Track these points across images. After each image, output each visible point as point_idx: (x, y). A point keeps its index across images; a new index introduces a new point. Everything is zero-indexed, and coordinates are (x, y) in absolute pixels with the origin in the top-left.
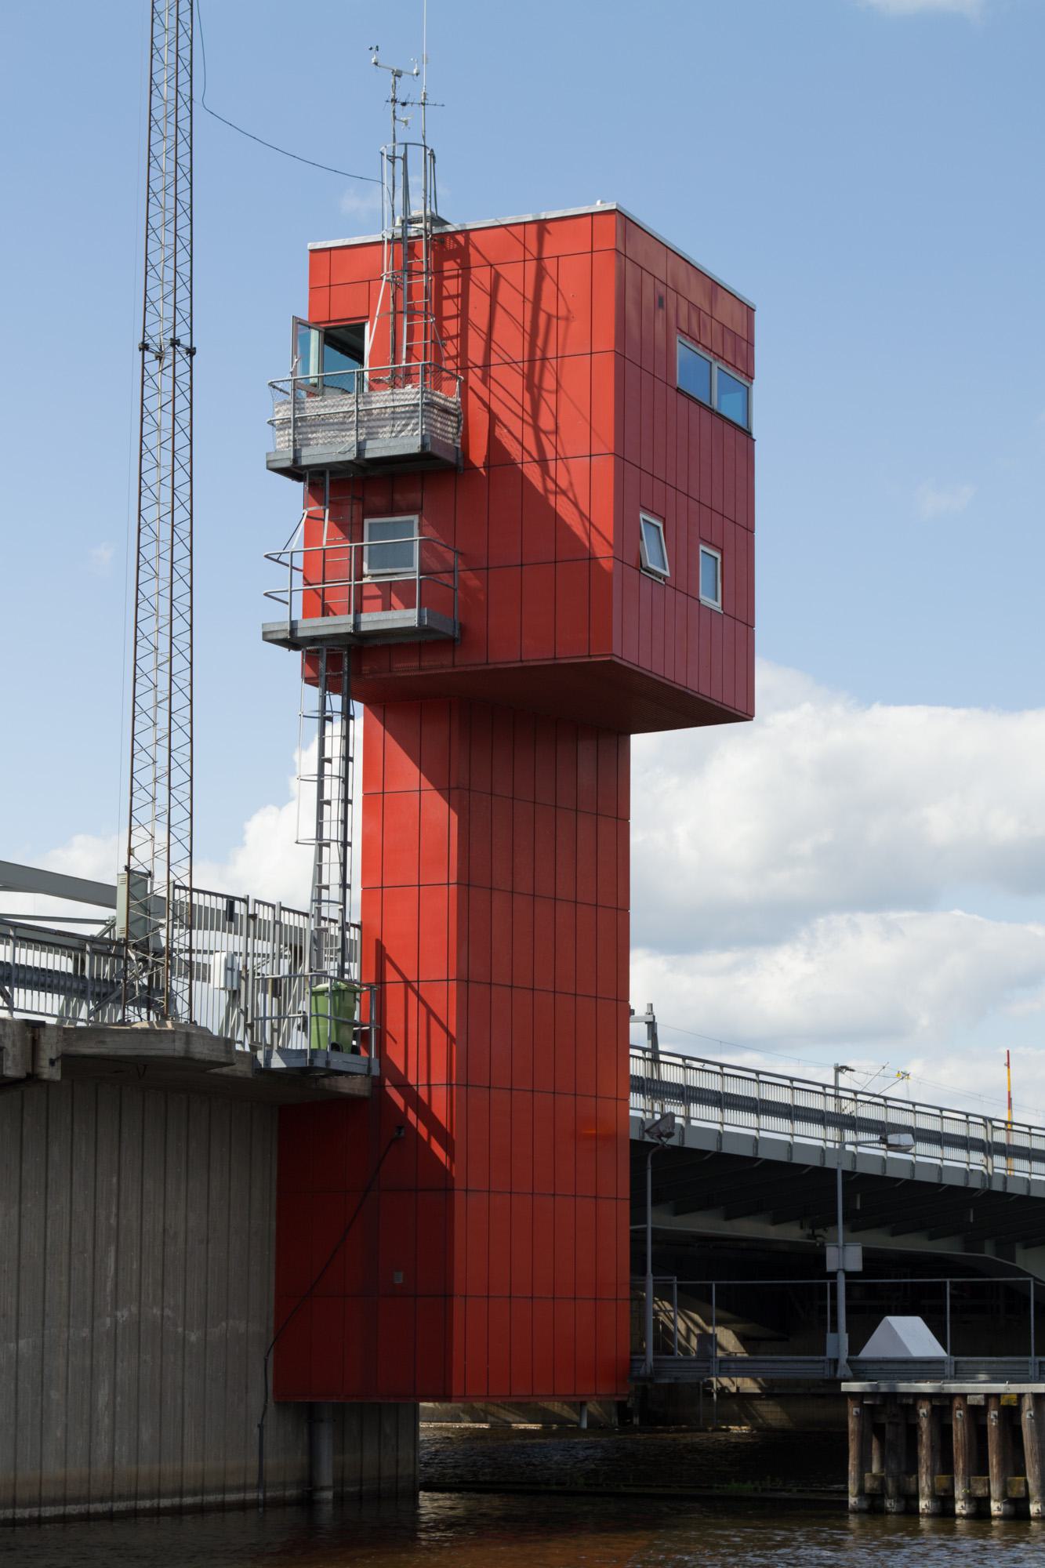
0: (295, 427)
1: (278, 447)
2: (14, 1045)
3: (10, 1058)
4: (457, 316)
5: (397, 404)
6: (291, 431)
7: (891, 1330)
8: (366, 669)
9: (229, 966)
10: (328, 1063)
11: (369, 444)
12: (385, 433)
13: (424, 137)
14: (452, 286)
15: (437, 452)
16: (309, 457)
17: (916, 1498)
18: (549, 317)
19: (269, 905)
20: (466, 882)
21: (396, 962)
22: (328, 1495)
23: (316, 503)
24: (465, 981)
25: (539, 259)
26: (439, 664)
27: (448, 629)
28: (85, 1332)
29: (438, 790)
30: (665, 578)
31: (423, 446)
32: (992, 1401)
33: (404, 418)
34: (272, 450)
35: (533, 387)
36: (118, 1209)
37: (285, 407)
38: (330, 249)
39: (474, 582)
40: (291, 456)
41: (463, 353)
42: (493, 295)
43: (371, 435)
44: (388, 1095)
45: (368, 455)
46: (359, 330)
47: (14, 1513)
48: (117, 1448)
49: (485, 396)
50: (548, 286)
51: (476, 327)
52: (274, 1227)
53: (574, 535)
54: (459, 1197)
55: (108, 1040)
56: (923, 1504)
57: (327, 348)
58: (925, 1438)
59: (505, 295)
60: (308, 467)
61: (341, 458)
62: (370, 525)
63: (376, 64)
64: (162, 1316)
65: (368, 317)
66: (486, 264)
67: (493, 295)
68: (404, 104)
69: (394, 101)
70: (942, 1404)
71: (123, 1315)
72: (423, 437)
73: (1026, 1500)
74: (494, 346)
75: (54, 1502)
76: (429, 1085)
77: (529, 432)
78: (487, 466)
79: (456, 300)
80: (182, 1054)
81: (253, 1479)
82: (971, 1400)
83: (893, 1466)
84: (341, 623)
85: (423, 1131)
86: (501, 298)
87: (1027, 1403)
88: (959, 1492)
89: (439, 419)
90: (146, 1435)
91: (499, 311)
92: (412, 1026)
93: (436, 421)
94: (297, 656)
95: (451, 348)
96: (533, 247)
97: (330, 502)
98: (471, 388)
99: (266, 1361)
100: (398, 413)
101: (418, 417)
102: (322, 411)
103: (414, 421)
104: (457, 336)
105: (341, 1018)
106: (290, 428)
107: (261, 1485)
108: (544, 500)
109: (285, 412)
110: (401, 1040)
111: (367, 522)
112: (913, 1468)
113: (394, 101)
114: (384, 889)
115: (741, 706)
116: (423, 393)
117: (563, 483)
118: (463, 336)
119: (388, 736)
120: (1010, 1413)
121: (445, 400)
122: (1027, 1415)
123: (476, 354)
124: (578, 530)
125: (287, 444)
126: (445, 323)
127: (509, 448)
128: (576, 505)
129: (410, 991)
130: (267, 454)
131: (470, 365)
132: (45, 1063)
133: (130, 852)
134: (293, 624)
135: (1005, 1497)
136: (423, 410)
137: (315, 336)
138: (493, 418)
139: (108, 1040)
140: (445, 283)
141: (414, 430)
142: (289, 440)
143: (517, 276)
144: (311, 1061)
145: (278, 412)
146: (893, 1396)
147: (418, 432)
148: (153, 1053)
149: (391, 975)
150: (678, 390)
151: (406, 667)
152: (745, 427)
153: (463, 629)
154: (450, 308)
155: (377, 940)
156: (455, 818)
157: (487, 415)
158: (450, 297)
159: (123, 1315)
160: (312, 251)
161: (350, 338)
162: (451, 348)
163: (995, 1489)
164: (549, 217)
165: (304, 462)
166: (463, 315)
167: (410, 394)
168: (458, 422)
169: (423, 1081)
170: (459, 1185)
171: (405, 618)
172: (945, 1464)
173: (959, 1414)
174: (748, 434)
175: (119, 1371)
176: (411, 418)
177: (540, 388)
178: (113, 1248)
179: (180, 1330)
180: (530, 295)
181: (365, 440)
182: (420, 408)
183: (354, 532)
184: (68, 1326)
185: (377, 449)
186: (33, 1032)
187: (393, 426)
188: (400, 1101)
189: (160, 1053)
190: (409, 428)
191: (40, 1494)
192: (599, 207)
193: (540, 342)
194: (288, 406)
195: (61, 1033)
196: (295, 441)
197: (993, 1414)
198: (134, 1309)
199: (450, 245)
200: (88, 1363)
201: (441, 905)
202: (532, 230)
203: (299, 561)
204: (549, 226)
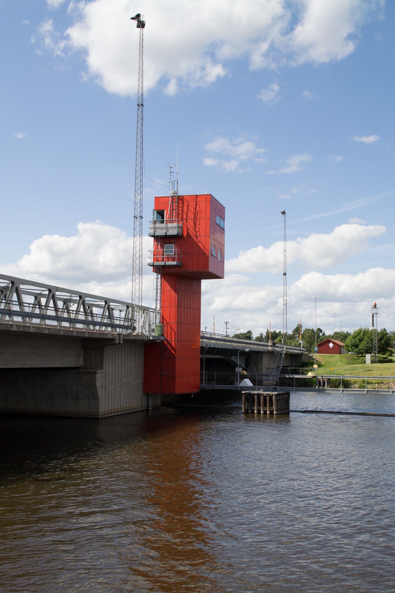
7: (246, 382)
8: (164, 270)
12: (170, 231)
14: (181, 205)
16: (157, 234)
17: (254, 410)
18: (198, 211)
20: (178, 306)
22: (151, 408)
24: (178, 323)
25: (196, 202)
26: (178, 270)
27: (180, 265)
28: (120, 384)
29: (174, 290)
32: (268, 395)
35: (195, 224)
39: (184, 256)
43: (168, 231)
45: (167, 234)
46: (164, 211)
49: (186, 224)
50: (198, 207)
51: (185, 213)
53: (202, 250)
54: (177, 359)
55: (131, 336)
56: (255, 412)
58: (256, 401)
61: (162, 235)
70: (259, 395)
71: (125, 380)
73: (273, 411)
75: (116, 413)
77: (194, 231)
80: (142, 339)
81: (140, 406)
82: (264, 395)
83: (250, 405)
84: (162, 263)
85: (170, 348)
87: (274, 396)
88: (262, 410)
90: (128, 400)
91: (189, 210)
94: (152, 267)
95: (180, 216)
96: (195, 200)
107: (142, 407)
108: (196, 243)
111: (165, 245)
112: (253, 405)
115: (218, 274)
117: (200, 240)
118: (182, 214)
119: (165, 281)
120: (271, 397)
122: (274, 398)
123: (185, 217)
124: (203, 248)
128: (202, 244)
135: (270, 410)
137: (155, 212)
138: (188, 229)
139: (131, 336)
143: (192, 204)
146: (250, 394)
147: (176, 231)
150: (217, 224)
151: (172, 271)
152: (223, 228)
153: (182, 264)
154: (180, 209)
156: (176, 295)
158: (180, 207)
159: (125, 380)
160: (155, 197)
161: (162, 213)
162: (180, 216)
163: (268, 409)
165: (156, 235)
166: (183, 210)
167: (175, 224)
169: (170, 340)
170: (177, 358)
171: (174, 263)
172: (259, 405)
173: (262, 397)
174: (224, 230)
177: (196, 224)
180: (195, 208)
183: (162, 247)
185: (168, 234)
188: (166, 343)
192: (206, 193)
193: (196, 216)
197: (268, 397)
199: (180, 198)
201: (174, 310)
202: (195, 196)
203: (152, 251)
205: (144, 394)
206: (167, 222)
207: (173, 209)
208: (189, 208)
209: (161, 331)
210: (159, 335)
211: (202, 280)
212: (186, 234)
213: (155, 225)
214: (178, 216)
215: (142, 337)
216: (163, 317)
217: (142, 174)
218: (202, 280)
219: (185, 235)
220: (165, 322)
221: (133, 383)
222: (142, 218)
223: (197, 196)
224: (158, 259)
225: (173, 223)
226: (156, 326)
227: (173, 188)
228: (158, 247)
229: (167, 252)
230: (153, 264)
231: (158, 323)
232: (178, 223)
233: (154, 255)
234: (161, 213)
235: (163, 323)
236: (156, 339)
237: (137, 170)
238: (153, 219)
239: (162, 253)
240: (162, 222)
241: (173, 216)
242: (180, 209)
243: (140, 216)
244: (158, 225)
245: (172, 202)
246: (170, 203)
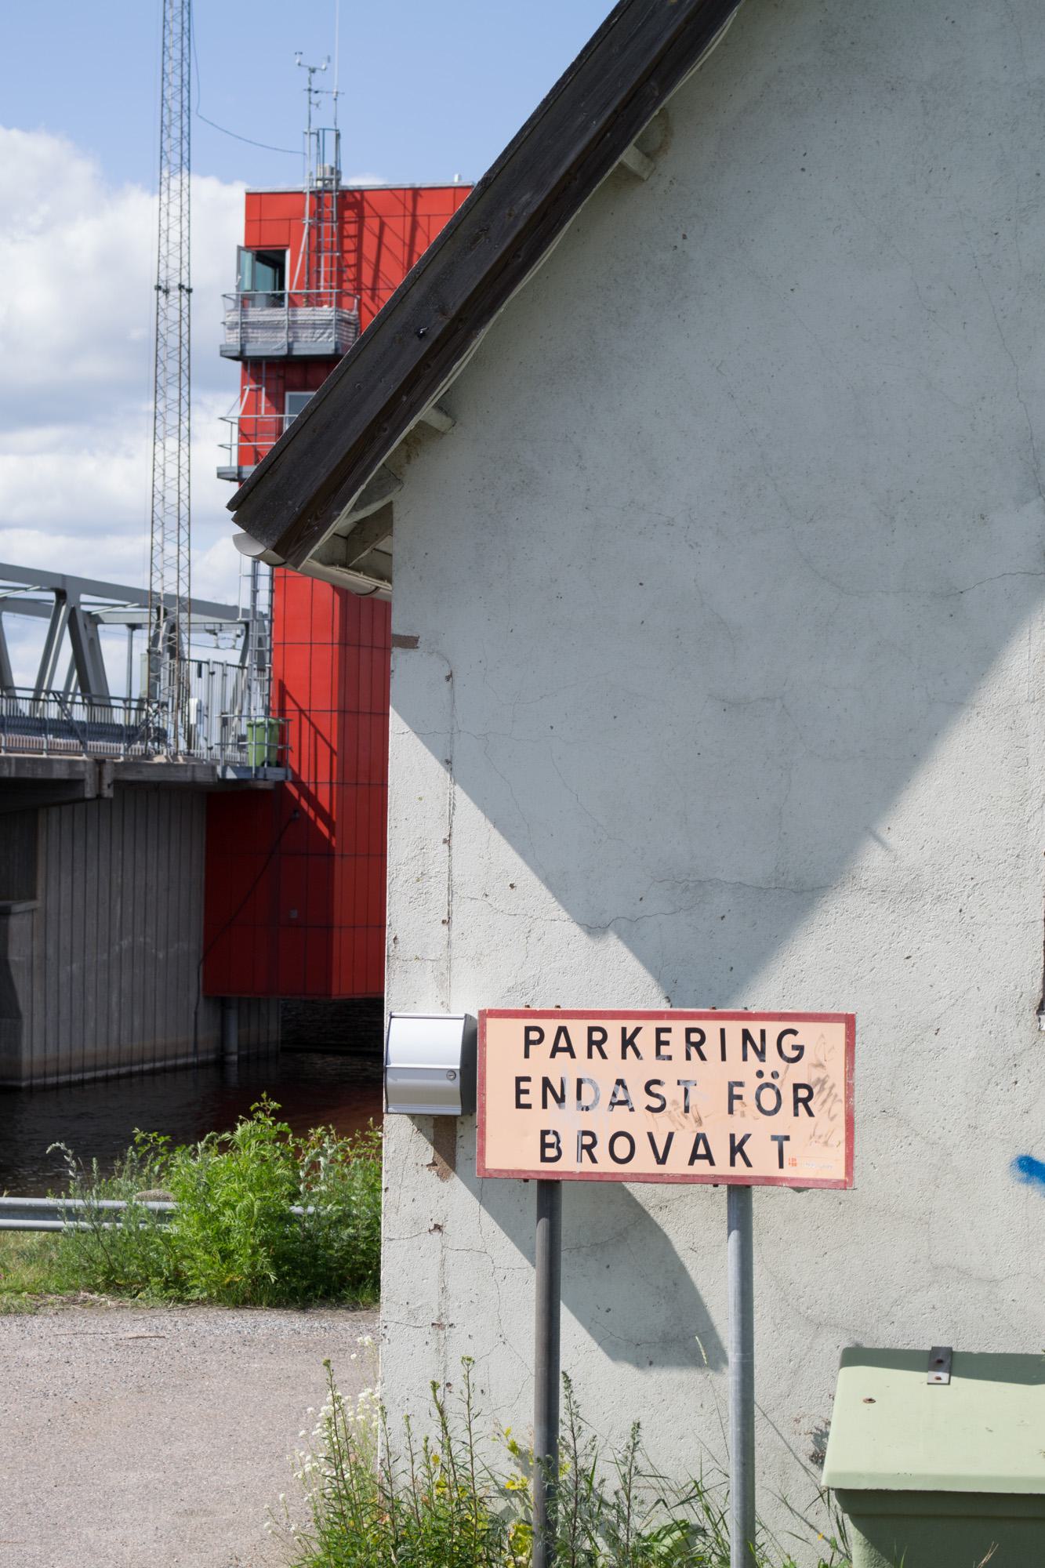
0: (242, 328)
1: (228, 341)
2: (90, 777)
3: (89, 786)
4: (354, 251)
5: (317, 318)
6: (238, 330)
10: (265, 775)
11: (296, 345)
13: (335, 123)
14: (351, 229)
16: (252, 350)
19: (220, 663)
20: (344, 643)
21: (294, 697)
22: (235, 1058)
23: (251, 381)
24: (343, 712)
25: (414, 215)
28: (105, 956)
33: (321, 329)
34: (223, 343)
37: (234, 313)
38: (261, 194)
40: (239, 349)
41: (358, 279)
42: (380, 238)
43: (296, 338)
44: (286, 788)
45: (295, 353)
46: (283, 253)
47: (71, 1078)
48: (122, 1033)
52: (203, 877)
54: (337, 859)
55: (144, 770)
57: (259, 265)
59: (388, 238)
60: (250, 357)
62: (290, 396)
63: (299, 64)
64: (145, 943)
65: (288, 246)
66: (374, 215)
67: (380, 238)
68: (316, 92)
69: (310, 90)
71: (125, 943)
72: (336, 343)
74: (381, 275)
75: (90, 1070)
76: (316, 783)
79: (353, 239)
81: (191, 1050)
85: (312, 814)
86: (386, 240)
89: (346, 329)
90: (137, 1023)
91: (384, 251)
92: (305, 741)
93: (343, 331)
95: (350, 274)
96: (411, 210)
97: (266, 379)
98: (364, 304)
99: (199, 968)
100: (318, 324)
101: (332, 328)
102: (261, 319)
103: (329, 331)
104: (354, 265)
105: (272, 744)
106: (237, 328)
107: (196, 1053)
109: (235, 317)
110: (296, 749)
111: (288, 394)
113: (310, 90)
114: (286, 645)
116: (336, 311)
118: (358, 266)
121: (349, 315)
125: (235, 340)
129: (303, 717)
131: (364, 287)
132: (105, 787)
136: (336, 324)
137: (248, 257)
139: (144, 770)
140: (346, 226)
141: (329, 337)
142: (237, 337)
143: (398, 226)
144: (256, 775)
145: (228, 316)
148: (172, 779)
154: (349, 244)
155: (280, 681)
158: (349, 237)
162: (350, 274)
164: (423, 186)
165: (248, 353)
166: (359, 250)
167: (326, 312)
168: (356, 329)
169: (312, 780)
170: (337, 852)
175: (123, 981)
176: (326, 329)
178: (119, 900)
179: (154, 951)
180: (407, 241)
181: (293, 342)
182: (334, 322)
184: (97, 953)
185: (300, 350)
186: (100, 767)
187: (314, 333)
188: (295, 793)
189: (177, 779)
190: (326, 335)
191: (83, 1065)
194: (236, 313)
196: (241, 338)
198: (130, 938)
199: (350, 199)
200: (106, 976)
201: (327, 658)
202: (410, 194)
203: (236, 421)
204: (421, 192)
205: (206, 998)
206: (297, 300)
207: (319, 243)
209: (269, 748)
210: (263, 765)
213: (244, 314)
214: (340, 272)
215: (189, 774)
216: (283, 691)
217: (186, 110)
220: (290, 705)
221: (161, 955)
222: (189, 291)
223: (416, 192)
224: (259, 450)
225: (321, 305)
226: (250, 726)
227: (321, 156)
228: (258, 401)
230: (239, 474)
231: (261, 712)
232: (339, 304)
233: (244, 436)
234: (269, 258)
235: (282, 712)
236: (251, 780)
237: (168, 93)
238: (238, 287)
239: (274, 427)
240: (276, 301)
241: (319, 272)
242: (349, 244)
243: (181, 287)
244: (259, 314)
245: (318, 216)
246: (307, 220)
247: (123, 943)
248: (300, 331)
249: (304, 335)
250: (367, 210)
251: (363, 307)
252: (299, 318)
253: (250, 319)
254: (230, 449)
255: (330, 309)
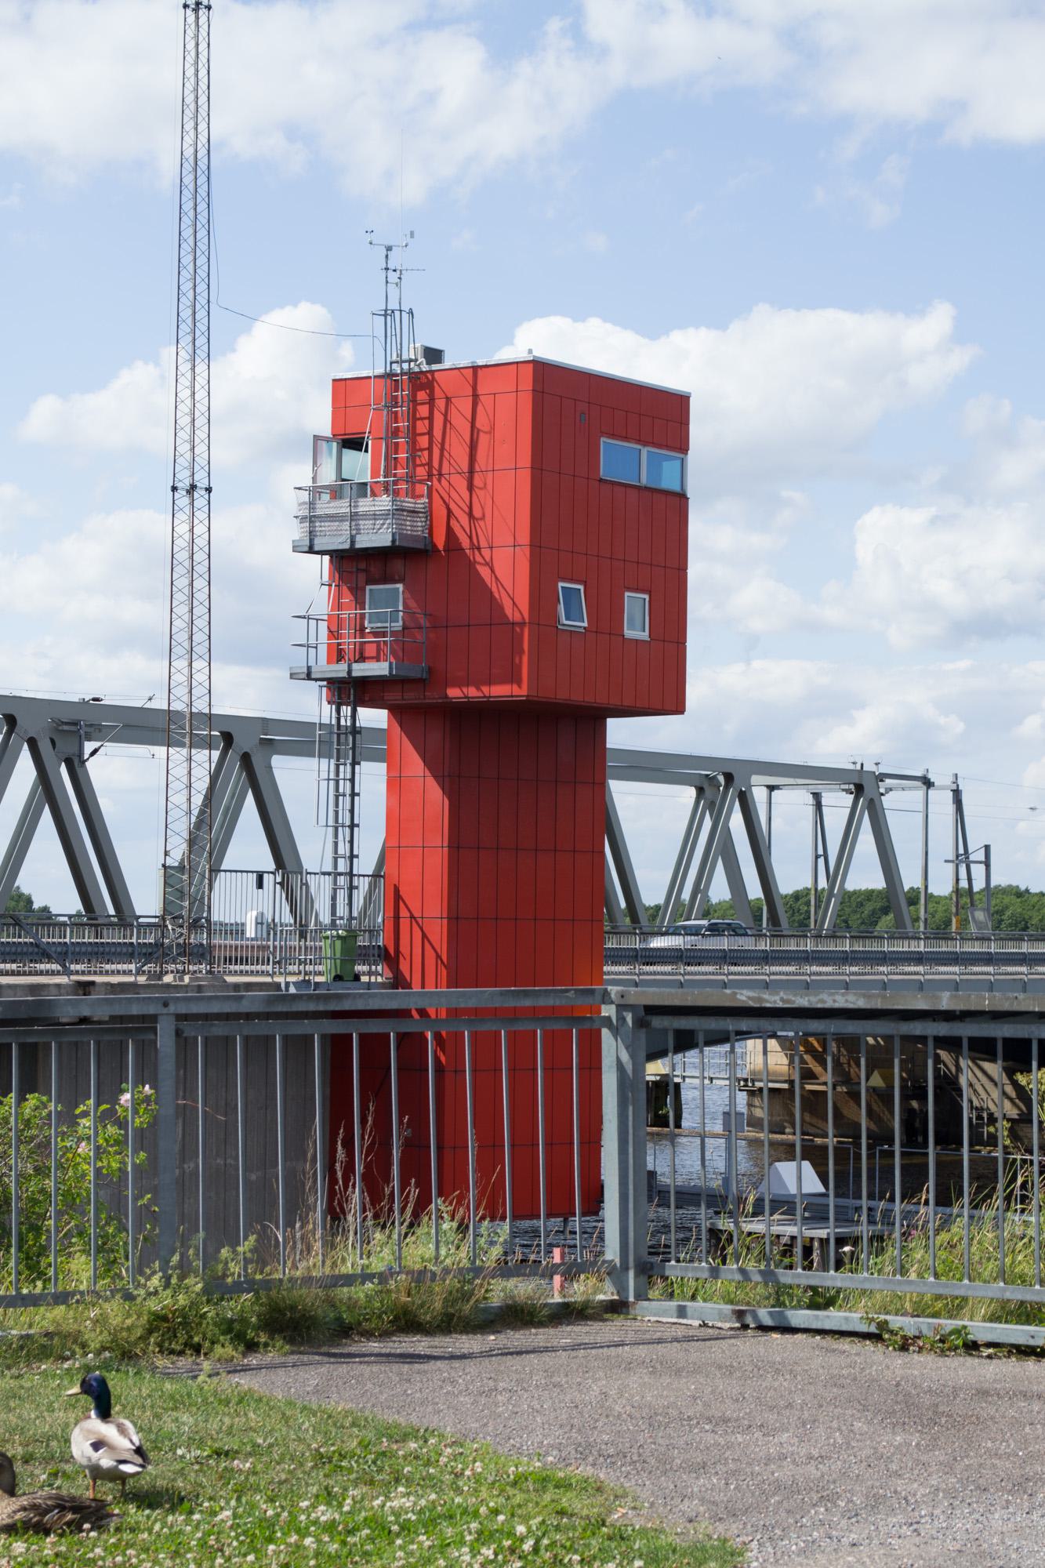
0: (310, 522)
9: (259, 921)
11: (358, 538)
14: (423, 410)
15: (405, 544)
21: (407, 903)
27: (415, 671)
29: (435, 777)
30: (585, 628)
31: (393, 541)
36: (185, 1092)
38: (346, 379)
40: (308, 543)
45: (358, 546)
62: (371, 590)
69: (387, 269)
78: (447, 549)
103: (388, 521)
110: (408, 958)
111: (368, 588)
113: (387, 269)
116: (393, 501)
126: (418, 438)
127: (459, 535)
130: (293, 541)
133: (166, 854)
134: (309, 668)
136: (393, 514)
138: (449, 512)
140: (419, 407)
141: (388, 528)
149: (404, 913)
153: (430, 670)
157: (445, 512)
160: (334, 380)
166: (430, 433)
175: (186, 1206)
185: (364, 541)
190: (385, 526)
195: (109, 988)
201: (438, 861)
208: (470, 425)
211: (609, 720)
212: (443, 538)
218: (609, 720)
219: (440, 541)
223: (475, 369)
229: (378, 617)
247: (186, 1166)
248: (361, 522)
249: (366, 525)
250: (438, 392)
251: (434, 493)
252: (360, 509)
253: (319, 512)
254: (316, 648)
255: (389, 498)
